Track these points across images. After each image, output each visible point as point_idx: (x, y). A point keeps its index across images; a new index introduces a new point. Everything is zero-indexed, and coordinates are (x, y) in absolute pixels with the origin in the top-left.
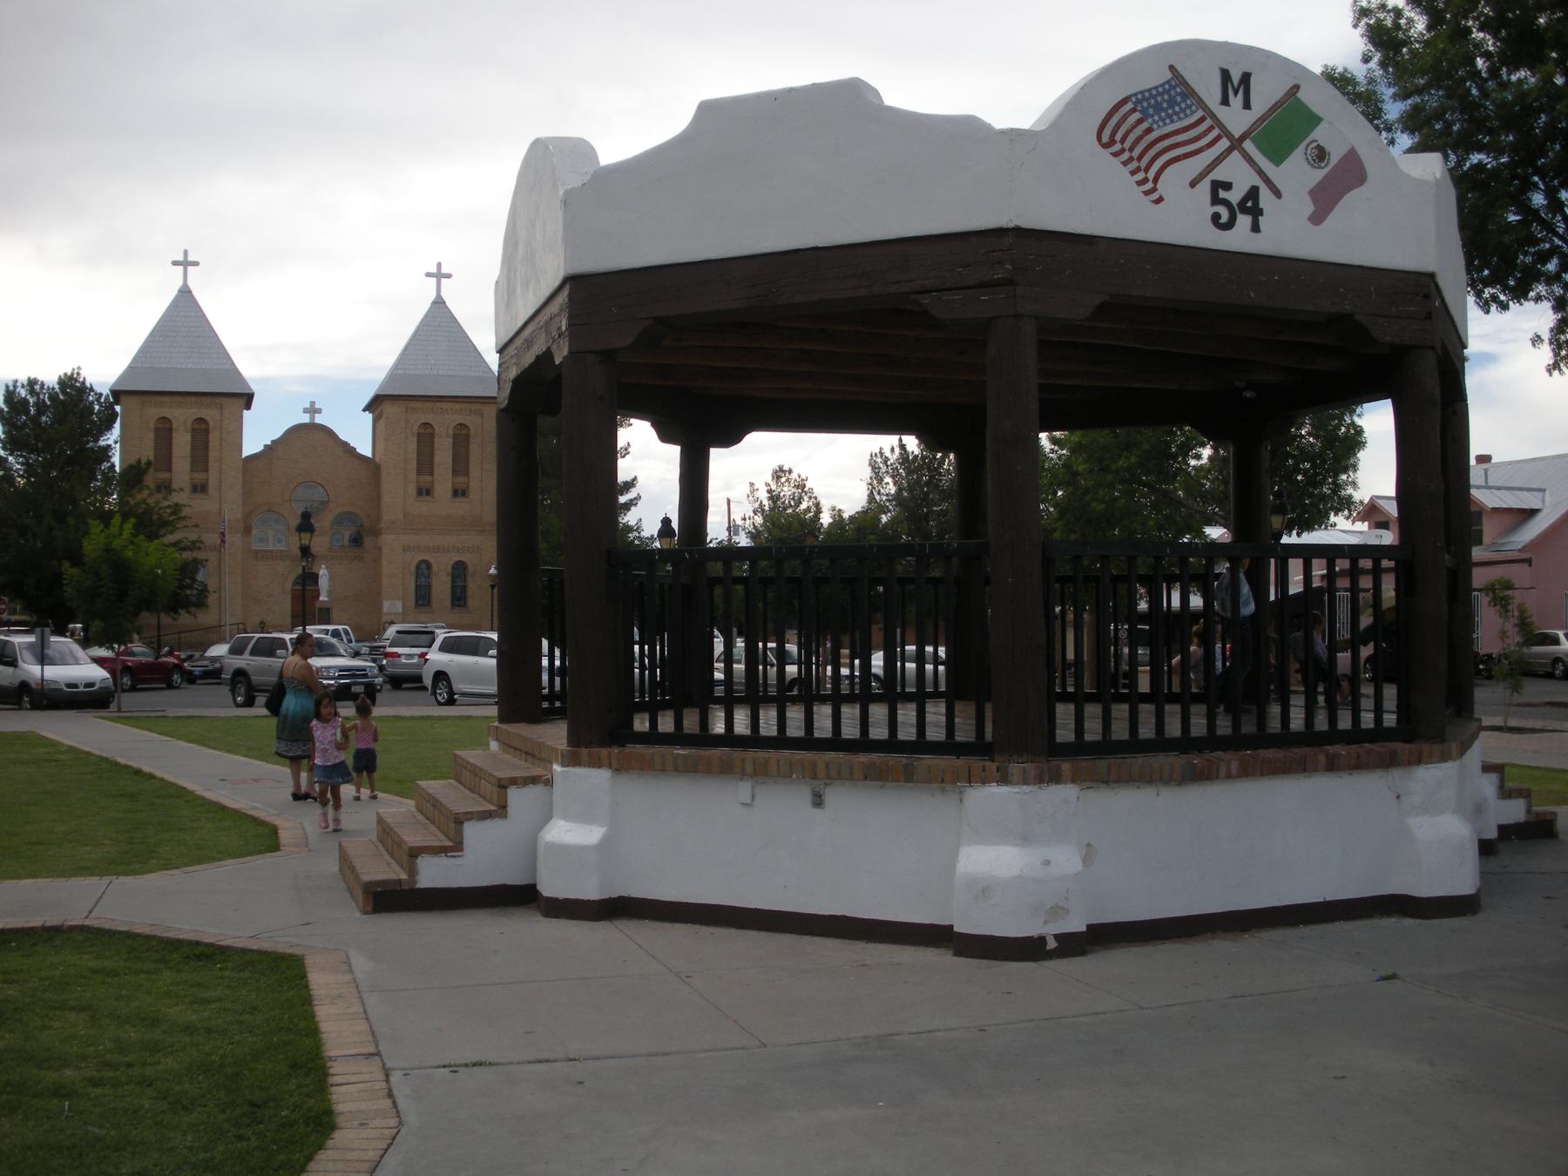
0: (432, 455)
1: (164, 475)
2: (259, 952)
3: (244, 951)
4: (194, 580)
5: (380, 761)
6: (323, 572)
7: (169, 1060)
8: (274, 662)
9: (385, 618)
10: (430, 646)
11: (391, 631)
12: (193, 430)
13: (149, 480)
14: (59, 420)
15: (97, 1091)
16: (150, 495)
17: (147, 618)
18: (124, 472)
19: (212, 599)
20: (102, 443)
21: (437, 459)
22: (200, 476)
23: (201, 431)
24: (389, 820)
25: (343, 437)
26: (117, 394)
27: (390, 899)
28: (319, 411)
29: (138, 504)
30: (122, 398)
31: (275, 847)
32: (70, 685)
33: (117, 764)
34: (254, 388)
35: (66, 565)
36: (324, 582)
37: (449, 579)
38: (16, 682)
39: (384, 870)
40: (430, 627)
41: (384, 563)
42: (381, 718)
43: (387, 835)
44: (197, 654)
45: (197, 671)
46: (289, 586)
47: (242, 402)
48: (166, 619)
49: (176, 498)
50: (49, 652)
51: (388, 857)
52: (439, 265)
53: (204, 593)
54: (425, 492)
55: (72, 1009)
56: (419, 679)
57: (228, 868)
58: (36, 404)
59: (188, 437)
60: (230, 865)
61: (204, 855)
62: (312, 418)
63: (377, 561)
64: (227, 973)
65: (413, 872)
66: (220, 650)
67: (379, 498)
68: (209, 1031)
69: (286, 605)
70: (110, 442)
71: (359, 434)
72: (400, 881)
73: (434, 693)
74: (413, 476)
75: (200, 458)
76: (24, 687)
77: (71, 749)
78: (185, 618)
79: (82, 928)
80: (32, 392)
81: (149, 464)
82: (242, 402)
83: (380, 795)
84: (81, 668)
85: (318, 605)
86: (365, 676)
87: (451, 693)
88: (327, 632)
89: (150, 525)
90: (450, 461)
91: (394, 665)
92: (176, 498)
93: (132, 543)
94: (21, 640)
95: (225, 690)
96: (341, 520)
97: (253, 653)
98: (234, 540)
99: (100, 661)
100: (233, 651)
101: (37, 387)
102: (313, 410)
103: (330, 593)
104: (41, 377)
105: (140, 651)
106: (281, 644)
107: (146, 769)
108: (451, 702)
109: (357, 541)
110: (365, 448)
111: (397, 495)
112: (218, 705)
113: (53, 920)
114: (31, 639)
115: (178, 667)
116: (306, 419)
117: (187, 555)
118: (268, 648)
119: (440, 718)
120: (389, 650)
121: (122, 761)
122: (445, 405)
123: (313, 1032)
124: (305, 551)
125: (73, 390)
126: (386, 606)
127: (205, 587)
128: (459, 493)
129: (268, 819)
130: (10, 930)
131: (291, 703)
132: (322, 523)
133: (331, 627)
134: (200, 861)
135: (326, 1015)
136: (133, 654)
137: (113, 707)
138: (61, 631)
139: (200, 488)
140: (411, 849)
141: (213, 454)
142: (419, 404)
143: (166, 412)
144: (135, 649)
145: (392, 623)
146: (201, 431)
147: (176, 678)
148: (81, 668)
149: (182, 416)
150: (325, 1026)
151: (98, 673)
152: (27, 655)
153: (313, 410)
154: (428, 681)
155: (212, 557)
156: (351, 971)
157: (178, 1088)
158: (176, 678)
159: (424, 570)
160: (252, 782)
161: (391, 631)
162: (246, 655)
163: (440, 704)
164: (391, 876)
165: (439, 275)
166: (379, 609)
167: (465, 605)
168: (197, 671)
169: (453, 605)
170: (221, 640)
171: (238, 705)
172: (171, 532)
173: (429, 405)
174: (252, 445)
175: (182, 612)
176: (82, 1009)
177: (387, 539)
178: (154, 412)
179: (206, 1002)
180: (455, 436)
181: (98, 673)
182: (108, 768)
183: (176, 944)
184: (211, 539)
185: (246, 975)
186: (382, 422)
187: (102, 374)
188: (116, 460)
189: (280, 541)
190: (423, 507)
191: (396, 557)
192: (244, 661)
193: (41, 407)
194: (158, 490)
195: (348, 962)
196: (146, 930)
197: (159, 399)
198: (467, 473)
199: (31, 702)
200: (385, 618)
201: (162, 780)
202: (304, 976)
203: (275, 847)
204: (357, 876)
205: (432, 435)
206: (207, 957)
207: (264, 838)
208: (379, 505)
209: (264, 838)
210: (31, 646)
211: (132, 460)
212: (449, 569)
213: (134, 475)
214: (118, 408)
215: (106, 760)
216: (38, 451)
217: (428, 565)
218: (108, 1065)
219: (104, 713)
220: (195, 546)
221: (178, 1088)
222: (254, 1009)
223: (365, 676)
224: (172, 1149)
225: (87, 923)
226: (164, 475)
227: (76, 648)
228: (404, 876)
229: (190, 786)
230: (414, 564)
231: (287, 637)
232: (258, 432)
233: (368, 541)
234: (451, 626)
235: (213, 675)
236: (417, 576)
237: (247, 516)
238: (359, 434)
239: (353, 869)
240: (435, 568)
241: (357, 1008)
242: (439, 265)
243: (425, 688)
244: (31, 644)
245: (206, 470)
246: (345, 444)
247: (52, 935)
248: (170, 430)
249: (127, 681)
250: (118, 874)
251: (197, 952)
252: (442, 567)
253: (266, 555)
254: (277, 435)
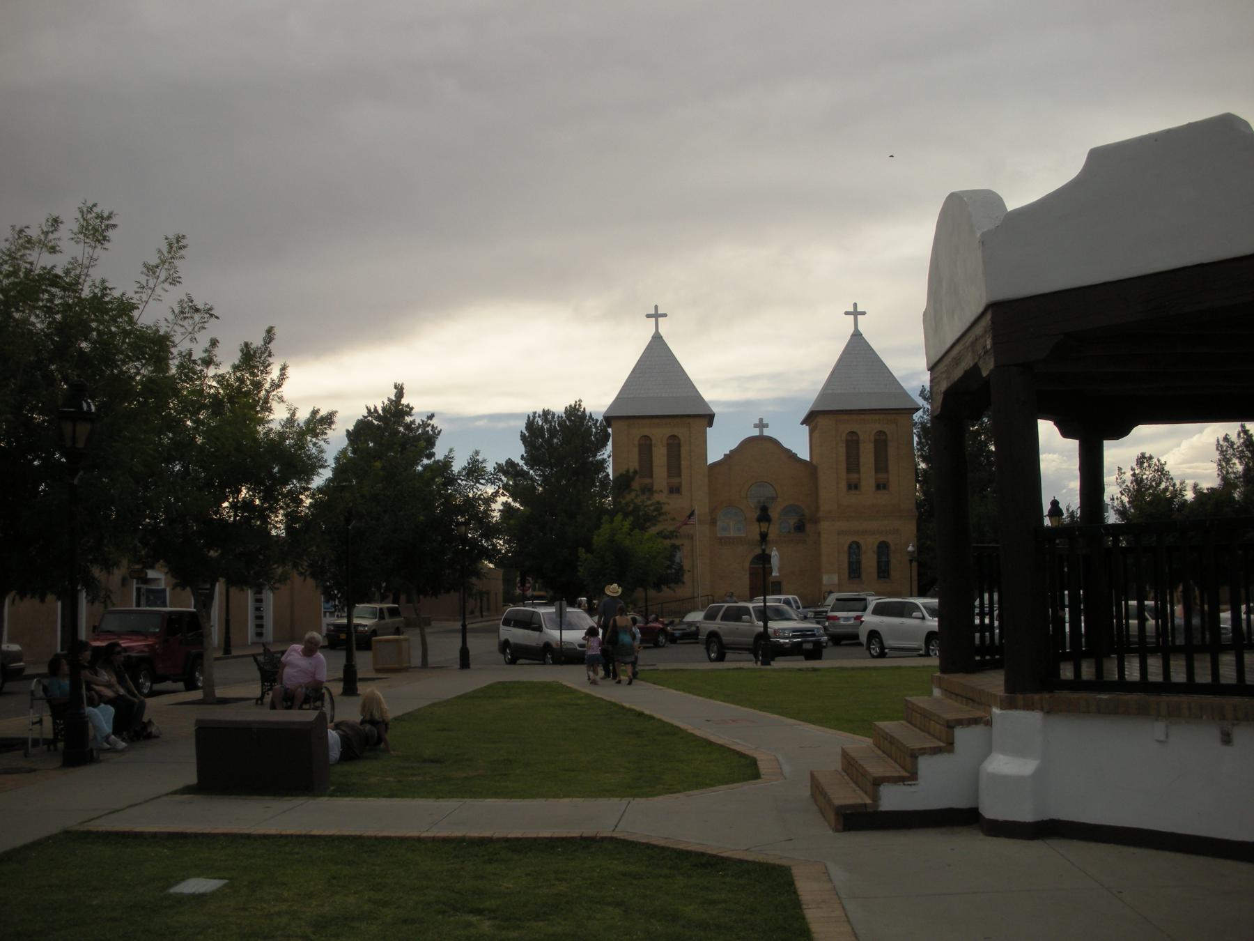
1: (647, 481)
2: (753, 863)
3: (741, 861)
6: (774, 554)
10: (864, 610)
11: (831, 600)
13: (636, 485)
18: (616, 479)
19: (687, 577)
20: (599, 458)
22: (675, 480)
26: (609, 419)
29: (627, 504)
31: (756, 776)
34: (715, 410)
37: (875, 556)
39: (848, 796)
44: (677, 620)
45: (677, 633)
46: (747, 565)
48: (652, 593)
49: (657, 497)
53: (680, 571)
54: (853, 486)
56: (856, 637)
57: (720, 792)
61: (700, 781)
64: (728, 879)
66: (696, 617)
69: (744, 581)
70: (605, 456)
73: (869, 648)
75: (674, 467)
78: (666, 592)
80: (546, 420)
81: (635, 472)
82: (706, 421)
85: (771, 580)
86: (814, 635)
87: (882, 648)
88: (779, 600)
89: (642, 520)
92: (657, 497)
95: (701, 649)
97: (723, 619)
100: (707, 617)
103: (780, 571)
106: (746, 611)
108: (882, 655)
109: (800, 527)
111: (831, 489)
112: (696, 660)
115: (663, 631)
117: (668, 543)
119: (875, 668)
120: (830, 614)
124: (764, 537)
125: (575, 414)
126: (826, 579)
129: (747, 752)
132: (774, 513)
134: (698, 785)
139: (675, 490)
141: (684, 463)
145: (830, 592)
146: (674, 445)
147: (662, 639)
149: (659, 435)
150: (814, 927)
154: (863, 639)
158: (662, 639)
159: (855, 550)
161: (831, 600)
162: (718, 621)
163: (873, 657)
168: (677, 633)
170: (694, 609)
171: (711, 660)
174: (715, 454)
175: (664, 588)
177: (825, 525)
178: (638, 432)
188: (610, 471)
191: (832, 538)
192: (717, 625)
193: (553, 432)
195: (827, 873)
196: (662, 843)
201: (660, 720)
202: (791, 884)
203: (756, 776)
207: (747, 768)
209: (747, 768)
211: (623, 471)
212: (875, 548)
213: (624, 482)
214: (610, 430)
217: (858, 545)
220: (672, 535)
223: (814, 635)
226: (647, 481)
231: (750, 605)
234: (877, 594)
235: (691, 636)
240: (864, 547)
243: (860, 644)
245: (679, 475)
248: (651, 445)
252: (869, 545)
254: (734, 446)
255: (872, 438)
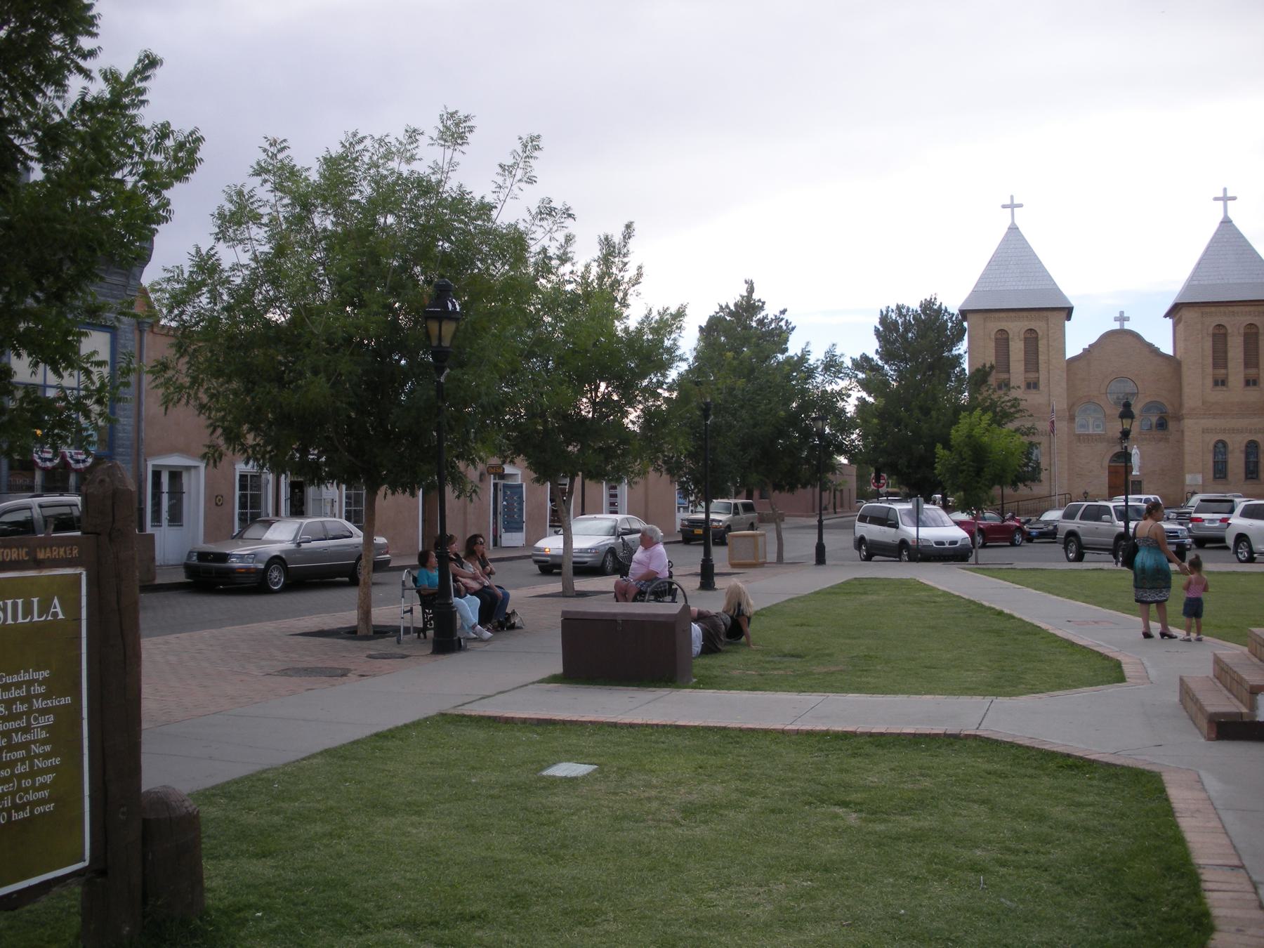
0: (1226, 352)
1: (1004, 376)
2: (1123, 767)
3: (1108, 765)
4: (1030, 460)
5: (1207, 607)
6: (1135, 451)
7: (1058, 851)
8: (1101, 525)
9: (1187, 489)
10: (1232, 511)
11: (1195, 500)
12: (1026, 339)
13: (992, 380)
14: (921, 335)
15: (1003, 870)
16: (995, 391)
17: (996, 490)
18: (972, 374)
19: (1043, 475)
20: (955, 352)
21: (1230, 355)
22: (1032, 375)
23: (1032, 339)
24: (1227, 660)
25: (1148, 339)
26: (964, 313)
27: (1229, 729)
28: (1127, 319)
29: (984, 400)
30: (969, 316)
31: (1121, 678)
32: (938, 543)
33: (983, 606)
34: (1073, 303)
35: (939, 446)
36: (1136, 460)
37: (1243, 456)
38: (898, 541)
39: (1223, 703)
40: (1229, 496)
41: (1187, 443)
42: (1210, 573)
43: (1223, 673)
44: (1034, 519)
45: (1034, 532)
46: (1106, 463)
47: (1064, 314)
48: (1008, 491)
49: (1014, 394)
50: (922, 517)
51: (1226, 692)
52: (1225, 190)
53: (1037, 469)
54: (1220, 382)
55: (974, 801)
56: (1222, 540)
57: (1084, 695)
58: (904, 323)
59: (1021, 345)
60: (1087, 691)
61: (1061, 683)
62: (1122, 325)
63: (1180, 441)
64: (1095, 782)
65: (1253, 707)
66: (1053, 515)
67: (1180, 389)
68: (1087, 830)
69: (1102, 480)
70: (961, 352)
71: (1162, 337)
72: (1241, 714)
73: (1236, 553)
74: (1210, 370)
75: (1032, 361)
76: (903, 543)
77: (945, 594)
78: (1023, 490)
79: (975, 737)
80: (900, 314)
81: (992, 367)
82: (1064, 314)
83: (1205, 638)
84: (945, 528)
85: (1131, 479)
86: (1177, 537)
87: (1251, 552)
88: (1140, 500)
89: (1001, 417)
90: (1242, 355)
91: (1198, 528)
92: (1014, 394)
93: (987, 430)
94: (901, 507)
95: (1059, 548)
96: (1148, 408)
97: (1081, 518)
98: (1062, 426)
99: (960, 524)
100: (1066, 516)
101: (904, 311)
102: (1122, 318)
103: (1141, 469)
104: (906, 304)
105: (990, 517)
106: (1106, 510)
107: (1006, 611)
108: (1251, 559)
109: (1162, 425)
110: (1167, 348)
111: (1196, 385)
112: (1053, 559)
113: (952, 729)
114: (909, 506)
115: (1020, 529)
116: (1116, 326)
117: (1025, 439)
118: (1095, 514)
119: (1244, 574)
120: (1194, 515)
121: (986, 604)
122: (1235, 309)
123: (1180, 840)
124: (1125, 434)
126: (1189, 479)
127: (1038, 464)
128: (1250, 382)
129: (1111, 655)
130: (921, 735)
131: (1144, 558)
132: (1136, 410)
133: (1143, 497)
134: (1061, 687)
135: (1187, 824)
136: (985, 519)
137: (972, 560)
138: (927, 501)
139: (1032, 385)
140: (1252, 687)
141: (1042, 358)
142: (1213, 309)
143: (1003, 325)
144: (987, 515)
145: (1194, 493)
146: (1032, 339)
147: (1018, 537)
148: (945, 528)
149: (1016, 328)
150: (1189, 836)
151: (960, 534)
152: (906, 519)
153: (1122, 318)
154: (1230, 542)
155: (1043, 440)
156: (1204, 789)
157: (1069, 876)
158: (1018, 537)
159: (1221, 448)
160: (1109, 628)
161: (1195, 500)
162: (1077, 520)
163: (1241, 561)
164: (1234, 710)
165: (1226, 199)
166: (1183, 481)
167: (1225, 477)
168: (1034, 532)
169: (1247, 478)
170: (1051, 508)
171: (1070, 560)
172: (1011, 421)
173: (1222, 309)
174: (1074, 348)
175: (1021, 485)
176: (983, 802)
177: (1188, 423)
178: (994, 325)
179: (1079, 805)
180: (1246, 335)
181: (960, 534)
182: (975, 610)
183: (1052, 755)
184: (1043, 426)
185: (1111, 785)
186: (1181, 326)
187: (953, 301)
188: (966, 366)
189: (1098, 426)
190: (1219, 395)
191: (1196, 438)
192: (1076, 524)
193: (907, 326)
194: (1000, 388)
195: (1200, 781)
196: (1027, 743)
197: (997, 315)
198: (1257, 366)
199: (909, 556)
200: (1187, 489)
201: (1020, 620)
202: (1162, 790)
203: (1121, 678)
204: (1201, 708)
205: (1225, 335)
206: (1077, 767)
207: (1112, 672)
208: (1180, 395)
209: (1112, 672)
210: (909, 512)
211: (979, 366)
212: (1243, 445)
213: (980, 377)
214: (965, 324)
215: (974, 603)
216: (906, 360)
217: (1224, 443)
218: (1009, 849)
219: (963, 565)
220: (1029, 432)
221: (1069, 876)
222: (1122, 815)
223: (1177, 537)
224: (1071, 927)
225: (979, 733)
226: (1004, 376)
227: (942, 513)
228: (1244, 710)
229: (1043, 626)
230: (1212, 443)
231: (1111, 505)
232: (1078, 338)
233: (1172, 425)
234: (1246, 495)
235: (1049, 535)
236: (1215, 455)
237: (1071, 407)
238: (1162, 337)
239: (1196, 701)
240: (1230, 447)
241: (1215, 823)
242: (1225, 190)
243: (1227, 548)
244: (909, 510)
245: (1038, 371)
246: (1150, 346)
247: (952, 740)
248: (1007, 339)
249: (979, 540)
250: (997, 695)
251: (1070, 761)
252: (1237, 445)
253: (1088, 439)
254: (1093, 340)
255: (1242, 331)
